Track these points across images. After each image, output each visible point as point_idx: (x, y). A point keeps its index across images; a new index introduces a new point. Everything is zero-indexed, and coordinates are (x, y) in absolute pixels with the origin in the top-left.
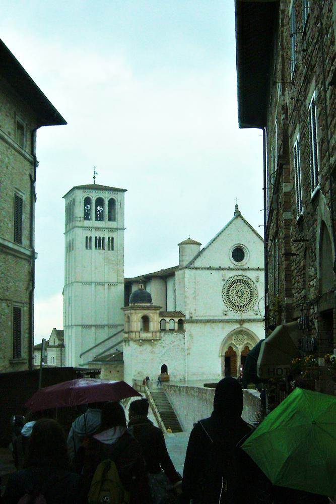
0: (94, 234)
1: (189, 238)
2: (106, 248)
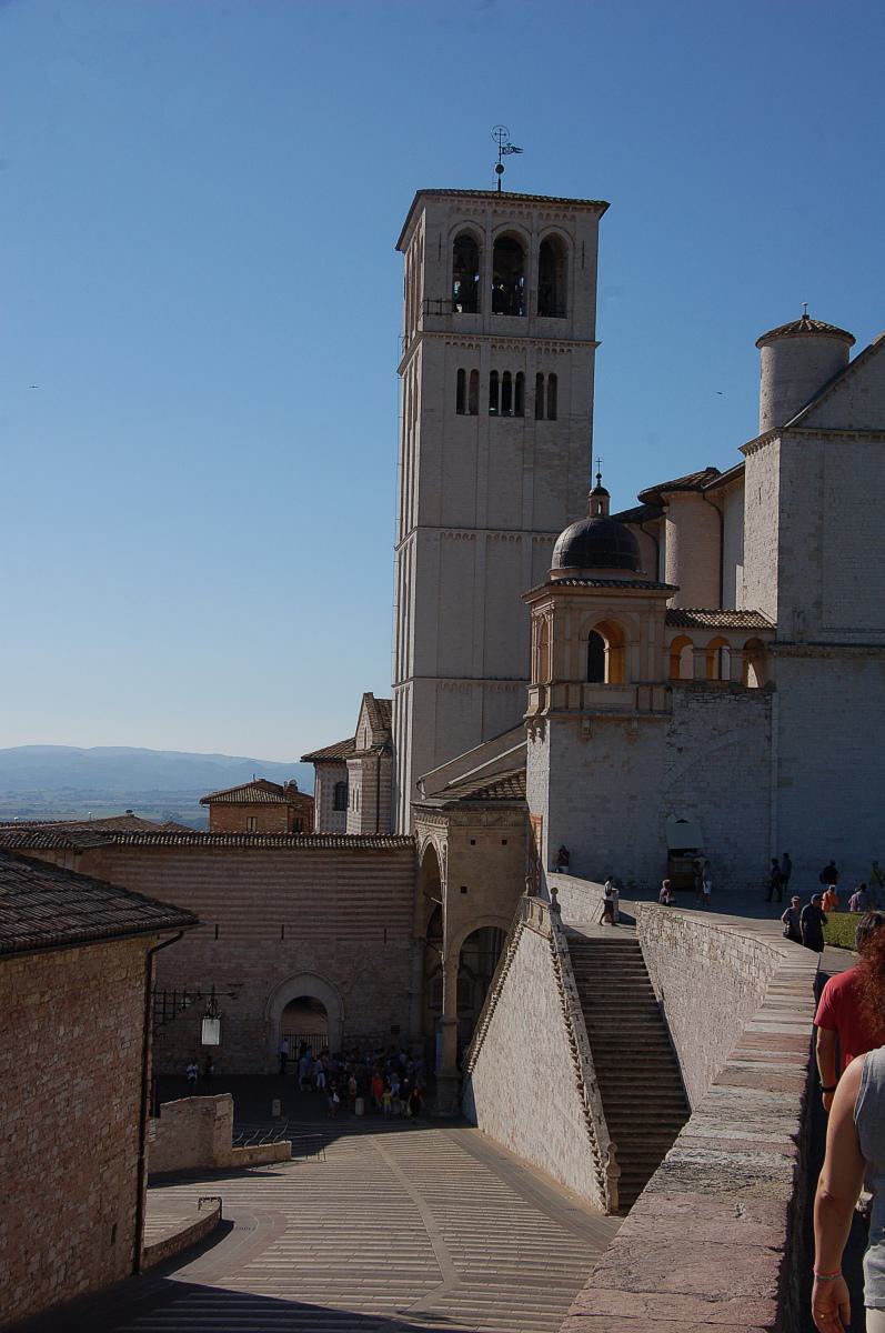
0: (487, 362)
1: (806, 317)
2: (529, 411)
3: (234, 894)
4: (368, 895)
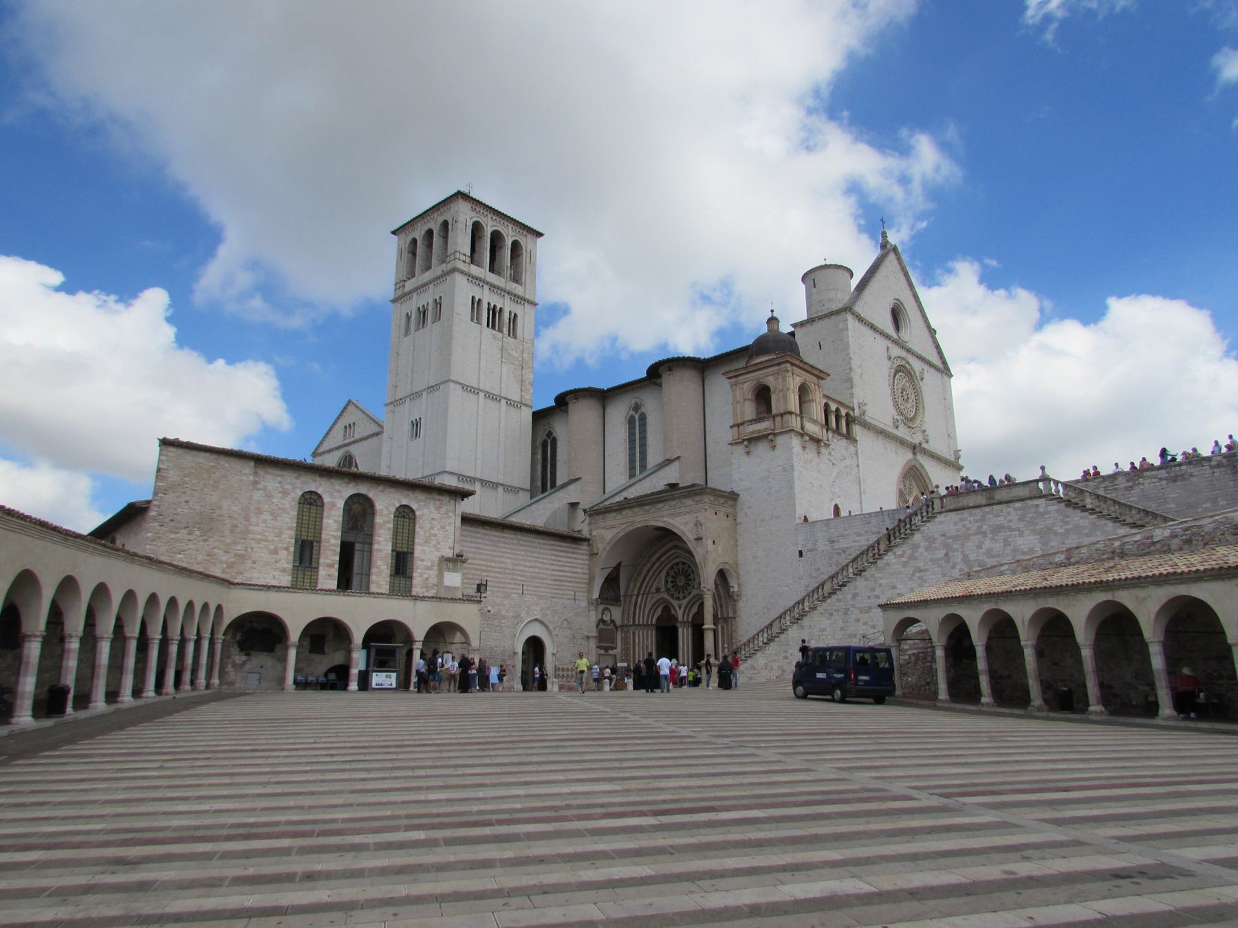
3: (496, 559)
4: (567, 569)
